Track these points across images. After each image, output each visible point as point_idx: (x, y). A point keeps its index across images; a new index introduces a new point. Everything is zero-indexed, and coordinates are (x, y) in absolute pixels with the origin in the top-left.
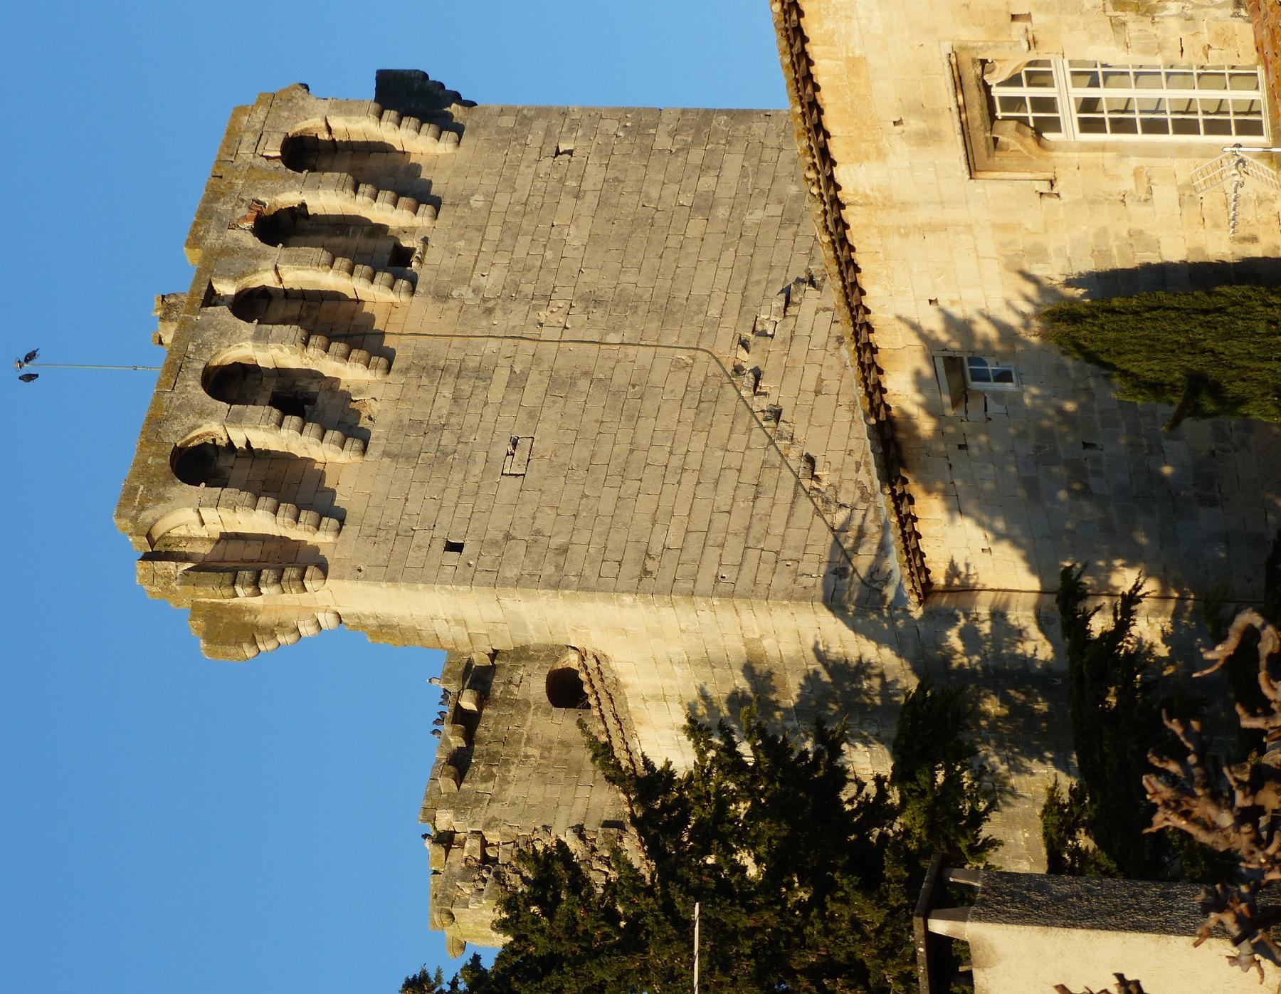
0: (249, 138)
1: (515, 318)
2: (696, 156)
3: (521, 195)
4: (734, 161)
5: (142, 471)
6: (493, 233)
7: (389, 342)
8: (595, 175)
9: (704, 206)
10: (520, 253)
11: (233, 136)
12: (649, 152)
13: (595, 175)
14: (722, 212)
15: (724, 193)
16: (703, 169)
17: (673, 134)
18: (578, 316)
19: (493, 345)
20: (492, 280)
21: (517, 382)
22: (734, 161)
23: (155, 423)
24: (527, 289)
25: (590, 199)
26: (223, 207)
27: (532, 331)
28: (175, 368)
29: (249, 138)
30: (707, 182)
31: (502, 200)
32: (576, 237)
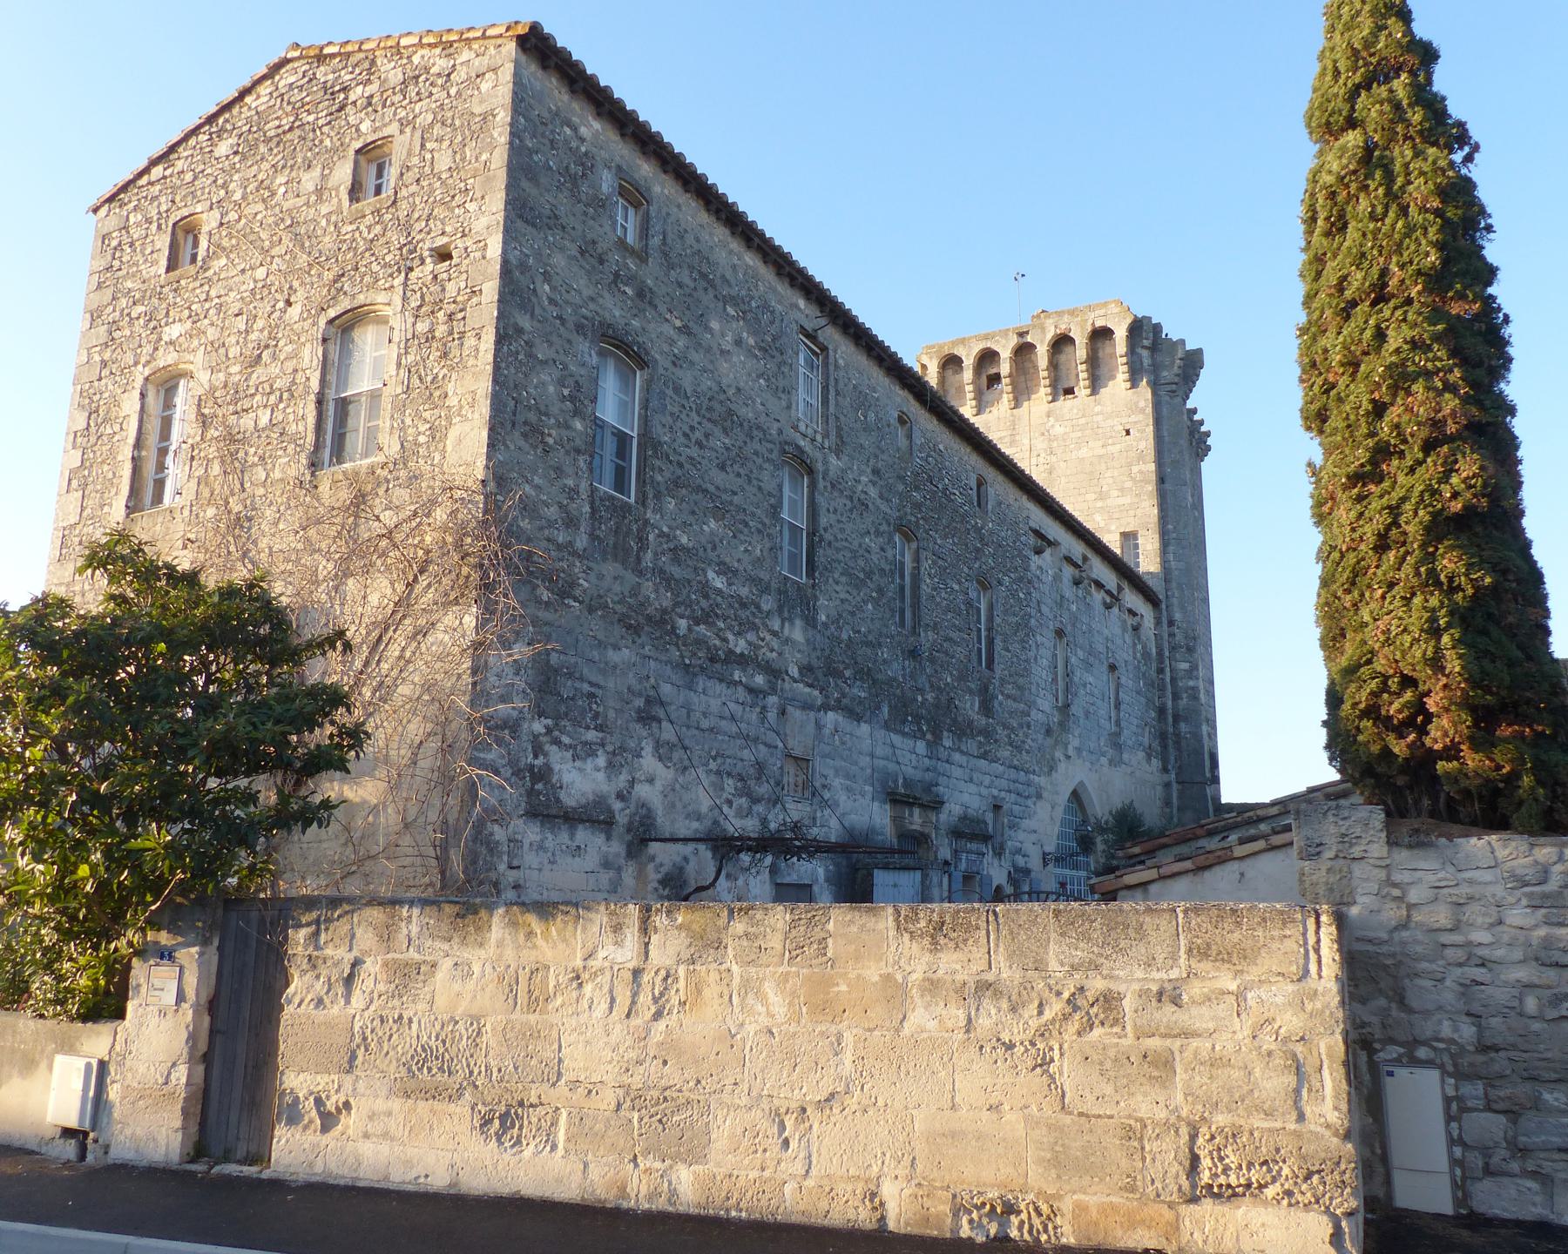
0: (1102, 312)
2: (1129, 484)
3: (1102, 424)
4: (1127, 500)
5: (941, 347)
6: (1082, 421)
7: (1026, 404)
8: (1115, 449)
9: (1102, 496)
11: (1105, 304)
12: (1130, 465)
13: (1115, 449)
14: (1099, 504)
15: (1109, 502)
16: (1122, 490)
17: (1140, 472)
18: (1041, 468)
19: (1026, 441)
20: (1058, 430)
22: (1127, 500)
23: (963, 341)
25: (1103, 451)
26: (1066, 318)
27: (1034, 453)
28: (986, 337)
29: (1102, 312)
30: (1116, 493)
31: (1100, 418)
32: (1084, 452)
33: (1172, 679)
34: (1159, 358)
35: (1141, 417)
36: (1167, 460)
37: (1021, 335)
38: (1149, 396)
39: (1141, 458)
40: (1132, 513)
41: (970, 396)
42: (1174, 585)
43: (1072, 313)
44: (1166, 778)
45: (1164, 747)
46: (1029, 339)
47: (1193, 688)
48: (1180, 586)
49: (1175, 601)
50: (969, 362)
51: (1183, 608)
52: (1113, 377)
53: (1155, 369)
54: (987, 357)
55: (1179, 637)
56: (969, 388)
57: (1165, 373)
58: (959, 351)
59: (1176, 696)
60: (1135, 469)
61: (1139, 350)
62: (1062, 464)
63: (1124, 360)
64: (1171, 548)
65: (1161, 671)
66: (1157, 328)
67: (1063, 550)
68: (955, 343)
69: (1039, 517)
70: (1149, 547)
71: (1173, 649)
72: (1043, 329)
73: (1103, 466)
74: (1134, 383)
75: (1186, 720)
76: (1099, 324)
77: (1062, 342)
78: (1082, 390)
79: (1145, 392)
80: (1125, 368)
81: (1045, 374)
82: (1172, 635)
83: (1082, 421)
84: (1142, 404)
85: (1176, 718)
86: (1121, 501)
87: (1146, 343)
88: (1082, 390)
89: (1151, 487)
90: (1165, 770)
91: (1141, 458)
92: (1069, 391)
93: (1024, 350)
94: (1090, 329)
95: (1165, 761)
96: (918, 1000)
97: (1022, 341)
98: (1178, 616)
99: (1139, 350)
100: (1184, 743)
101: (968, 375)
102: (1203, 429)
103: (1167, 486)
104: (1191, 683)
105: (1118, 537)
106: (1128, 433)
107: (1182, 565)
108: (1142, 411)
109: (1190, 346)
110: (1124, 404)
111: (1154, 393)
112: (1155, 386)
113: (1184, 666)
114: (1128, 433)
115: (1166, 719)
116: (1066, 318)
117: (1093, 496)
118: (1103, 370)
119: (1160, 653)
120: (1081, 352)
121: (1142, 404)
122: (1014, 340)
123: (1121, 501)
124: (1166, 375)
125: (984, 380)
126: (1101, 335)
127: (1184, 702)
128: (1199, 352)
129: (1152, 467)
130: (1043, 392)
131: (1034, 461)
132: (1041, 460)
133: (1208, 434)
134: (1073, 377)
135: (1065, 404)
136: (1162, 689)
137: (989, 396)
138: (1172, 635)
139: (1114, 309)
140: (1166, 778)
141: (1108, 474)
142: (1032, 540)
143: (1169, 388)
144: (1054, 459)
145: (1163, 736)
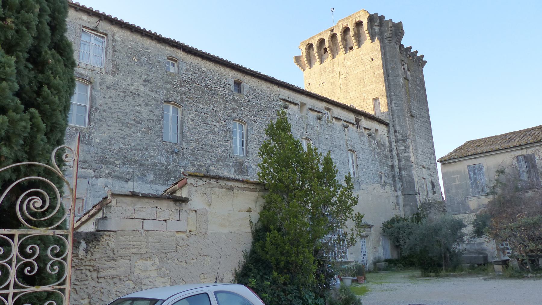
0: (358, 15)
1: (343, 70)
2: (374, 79)
4: (374, 86)
5: (306, 41)
6: (356, 59)
8: (368, 67)
9: (365, 86)
10: (353, 65)
14: (364, 89)
15: (368, 88)
16: (372, 82)
18: (344, 79)
19: (338, 70)
21: (333, 77)
22: (374, 86)
23: (313, 38)
24: (347, 69)
25: (364, 69)
27: (341, 74)
29: (358, 15)
30: (370, 84)
33: (398, 154)
34: (383, 29)
35: (376, 53)
36: (389, 68)
37: (332, 31)
38: (379, 44)
39: (378, 68)
40: (376, 90)
41: (317, 57)
42: (396, 116)
43: (348, 18)
44: (396, 194)
45: (395, 181)
46: (334, 32)
47: (407, 156)
48: (398, 116)
49: (396, 122)
50: (315, 45)
51: (400, 125)
52: (366, 39)
53: (381, 33)
54: (322, 42)
55: (399, 137)
56: (316, 54)
57: (386, 34)
58: (312, 42)
59: (399, 160)
60: (376, 73)
61: (374, 27)
62: (351, 76)
63: (367, 32)
64: (393, 102)
65: (391, 151)
66: (382, 18)
67: (308, 106)
68: (310, 39)
69: (285, 93)
70: (383, 102)
71: (397, 141)
72: (338, 27)
73: (365, 74)
74: (373, 40)
75: (404, 169)
76: (357, 20)
77: (346, 30)
78: (355, 47)
79: (377, 42)
80: (368, 35)
81: (340, 43)
82: (396, 136)
83: (356, 59)
84: (377, 47)
85: (400, 169)
86: (372, 86)
87: (376, 24)
88: (355, 47)
89: (382, 79)
90: (396, 190)
91: (378, 68)
92: (351, 48)
93: (333, 36)
94: (354, 22)
95: (395, 187)
96: (365, 285)
97: (332, 33)
98: (398, 128)
99: (374, 27)
100: (404, 179)
101: (315, 49)
102: (418, 55)
103: (390, 78)
104: (406, 154)
105: (372, 100)
106: (373, 60)
107: (399, 108)
108: (377, 50)
109: (396, 21)
110: (371, 49)
111: (380, 43)
112: (382, 41)
113: (403, 148)
114: (373, 60)
115: (394, 170)
116: (346, 21)
117: (362, 87)
118: (362, 38)
119: (390, 144)
120: (352, 32)
121: (377, 47)
122: (329, 33)
123: (372, 86)
124: (386, 34)
125: (323, 50)
126: (359, 24)
127: (403, 162)
128: (400, 23)
129: (382, 71)
130: (342, 51)
131: (341, 77)
132: (343, 76)
133: (423, 56)
134: (351, 43)
135: (350, 53)
136: (392, 158)
137: (324, 56)
138: (396, 136)
139: (362, 13)
140: (396, 194)
141: (367, 77)
142: (282, 103)
143: (388, 39)
144: (347, 75)
145: (394, 177)
